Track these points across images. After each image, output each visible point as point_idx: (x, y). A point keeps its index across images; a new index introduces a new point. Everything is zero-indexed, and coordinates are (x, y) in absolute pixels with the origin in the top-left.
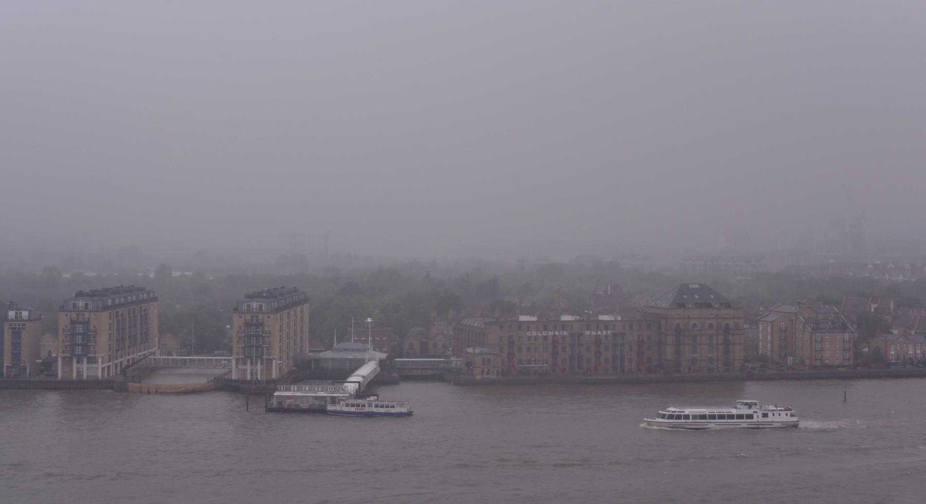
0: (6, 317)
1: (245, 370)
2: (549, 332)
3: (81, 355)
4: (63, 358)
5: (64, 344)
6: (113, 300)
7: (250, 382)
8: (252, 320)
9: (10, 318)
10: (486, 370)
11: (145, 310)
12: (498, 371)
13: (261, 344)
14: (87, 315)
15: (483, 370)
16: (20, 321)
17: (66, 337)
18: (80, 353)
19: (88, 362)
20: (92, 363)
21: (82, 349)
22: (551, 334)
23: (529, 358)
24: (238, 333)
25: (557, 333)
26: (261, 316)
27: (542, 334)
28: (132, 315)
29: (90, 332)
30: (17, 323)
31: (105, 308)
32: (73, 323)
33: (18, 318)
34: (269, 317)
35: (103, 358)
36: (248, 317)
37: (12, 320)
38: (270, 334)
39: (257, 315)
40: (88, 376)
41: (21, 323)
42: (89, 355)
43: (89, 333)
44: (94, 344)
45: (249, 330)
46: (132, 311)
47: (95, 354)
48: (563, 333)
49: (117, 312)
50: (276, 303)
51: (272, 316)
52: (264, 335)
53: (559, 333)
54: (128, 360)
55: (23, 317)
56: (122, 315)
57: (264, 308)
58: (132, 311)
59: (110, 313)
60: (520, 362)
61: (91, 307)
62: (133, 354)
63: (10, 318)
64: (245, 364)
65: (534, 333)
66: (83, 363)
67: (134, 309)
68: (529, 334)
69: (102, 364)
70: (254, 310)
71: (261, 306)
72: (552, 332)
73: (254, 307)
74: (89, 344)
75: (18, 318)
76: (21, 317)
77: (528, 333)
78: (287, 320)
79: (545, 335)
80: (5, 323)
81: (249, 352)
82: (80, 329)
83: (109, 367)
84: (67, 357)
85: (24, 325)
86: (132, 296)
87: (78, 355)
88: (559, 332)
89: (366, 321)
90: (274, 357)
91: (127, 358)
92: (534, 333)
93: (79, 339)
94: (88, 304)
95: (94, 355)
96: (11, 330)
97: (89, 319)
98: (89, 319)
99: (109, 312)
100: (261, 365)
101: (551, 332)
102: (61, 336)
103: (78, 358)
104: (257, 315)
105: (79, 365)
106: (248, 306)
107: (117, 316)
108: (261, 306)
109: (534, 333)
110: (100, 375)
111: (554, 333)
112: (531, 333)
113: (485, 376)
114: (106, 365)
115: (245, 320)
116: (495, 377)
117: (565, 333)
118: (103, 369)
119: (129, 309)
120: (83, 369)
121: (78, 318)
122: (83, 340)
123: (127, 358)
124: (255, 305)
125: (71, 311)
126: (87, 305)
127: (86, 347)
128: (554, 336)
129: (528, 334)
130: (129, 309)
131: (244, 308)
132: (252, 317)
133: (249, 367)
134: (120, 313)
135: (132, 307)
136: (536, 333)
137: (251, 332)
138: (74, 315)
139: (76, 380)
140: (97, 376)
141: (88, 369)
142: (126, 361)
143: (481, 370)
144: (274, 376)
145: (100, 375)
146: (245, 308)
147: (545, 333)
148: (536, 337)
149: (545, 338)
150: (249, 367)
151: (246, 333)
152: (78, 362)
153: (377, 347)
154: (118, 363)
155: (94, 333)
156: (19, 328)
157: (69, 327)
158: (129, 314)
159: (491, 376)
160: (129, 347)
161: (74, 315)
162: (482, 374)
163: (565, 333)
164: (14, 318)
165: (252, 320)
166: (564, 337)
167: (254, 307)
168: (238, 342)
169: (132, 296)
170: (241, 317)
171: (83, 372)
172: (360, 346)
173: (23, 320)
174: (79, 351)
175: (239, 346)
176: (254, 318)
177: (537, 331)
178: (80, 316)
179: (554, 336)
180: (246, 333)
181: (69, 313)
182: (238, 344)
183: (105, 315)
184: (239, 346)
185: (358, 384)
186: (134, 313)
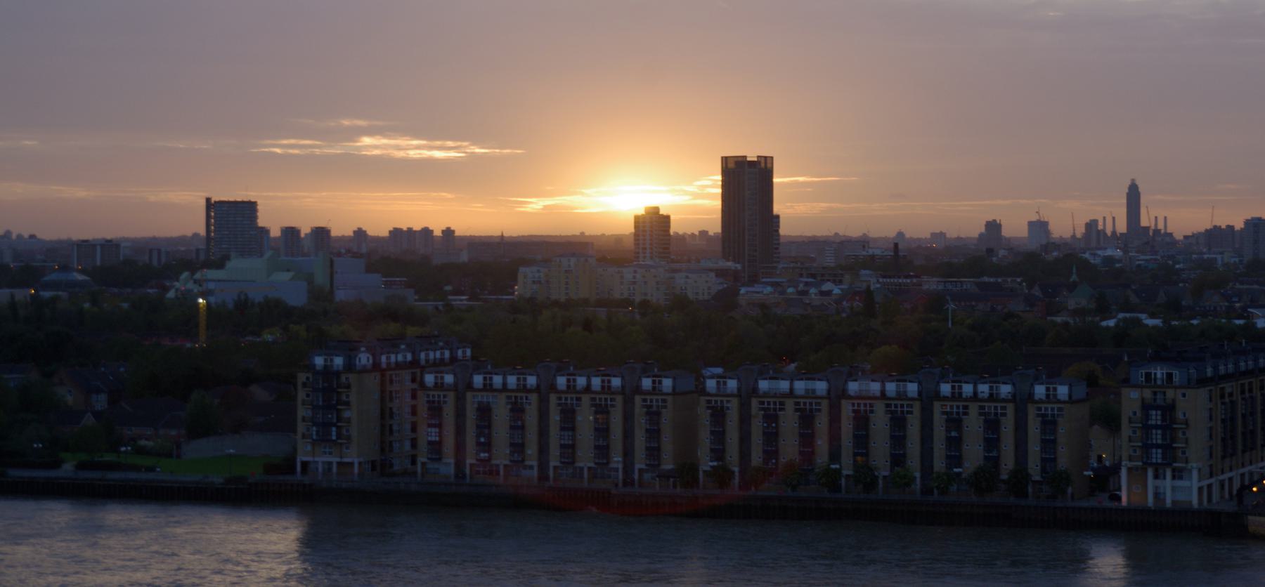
0: (1031, 395)
4: (1130, 470)
6: (1215, 368)
9: (1036, 397)
14: (1170, 393)
17: (1134, 432)
18: (1159, 461)
19: (1174, 477)
20: (1181, 478)
21: (1162, 453)
28: (1247, 395)
29: (1176, 424)
30: (1050, 406)
31: (1202, 382)
32: (1146, 407)
33: (1051, 397)
35: (1200, 470)
37: (1041, 401)
40: (1174, 502)
42: (1175, 465)
43: (1175, 426)
44: (1183, 445)
46: (1247, 387)
47: (1187, 462)
49: (1223, 389)
54: (1243, 475)
55: (1059, 397)
56: (1231, 395)
58: (1247, 387)
59: (1211, 390)
61: (1177, 380)
62: (1251, 464)
63: (1036, 397)
66: (1165, 478)
67: (1250, 383)
69: (1199, 481)
74: (1175, 445)
75: (1051, 397)
76: (1055, 396)
82: (1156, 417)
83: (1210, 486)
84: (1137, 468)
86: (1246, 362)
87: (1157, 464)
91: (1242, 471)
93: (1157, 437)
95: (1184, 465)
96: (1040, 419)
97: (1174, 400)
98: (1174, 400)
99: (1208, 388)
102: (1126, 431)
105: (1159, 482)
107: (1222, 396)
110: (1195, 502)
114: (1205, 483)
118: (1200, 489)
119: (1243, 385)
121: (1155, 400)
122: (1164, 438)
123: (1242, 471)
125: (1142, 387)
126: (1170, 376)
127: (1168, 448)
130: (1243, 385)
134: (1228, 390)
135: (1246, 381)
138: (1148, 394)
139: (1153, 508)
140: (1191, 502)
141: (1174, 489)
142: (1239, 477)
145: (1195, 502)
152: (1156, 477)
154: (1224, 480)
155: (1184, 426)
157: (1139, 414)
158: (1243, 392)
160: (1244, 452)
161: (1148, 394)
164: (1044, 397)
169: (1246, 362)
171: (1164, 493)
173: (1060, 402)
174: (1157, 456)
178: (1158, 396)
183: (1202, 394)
186: (1251, 390)
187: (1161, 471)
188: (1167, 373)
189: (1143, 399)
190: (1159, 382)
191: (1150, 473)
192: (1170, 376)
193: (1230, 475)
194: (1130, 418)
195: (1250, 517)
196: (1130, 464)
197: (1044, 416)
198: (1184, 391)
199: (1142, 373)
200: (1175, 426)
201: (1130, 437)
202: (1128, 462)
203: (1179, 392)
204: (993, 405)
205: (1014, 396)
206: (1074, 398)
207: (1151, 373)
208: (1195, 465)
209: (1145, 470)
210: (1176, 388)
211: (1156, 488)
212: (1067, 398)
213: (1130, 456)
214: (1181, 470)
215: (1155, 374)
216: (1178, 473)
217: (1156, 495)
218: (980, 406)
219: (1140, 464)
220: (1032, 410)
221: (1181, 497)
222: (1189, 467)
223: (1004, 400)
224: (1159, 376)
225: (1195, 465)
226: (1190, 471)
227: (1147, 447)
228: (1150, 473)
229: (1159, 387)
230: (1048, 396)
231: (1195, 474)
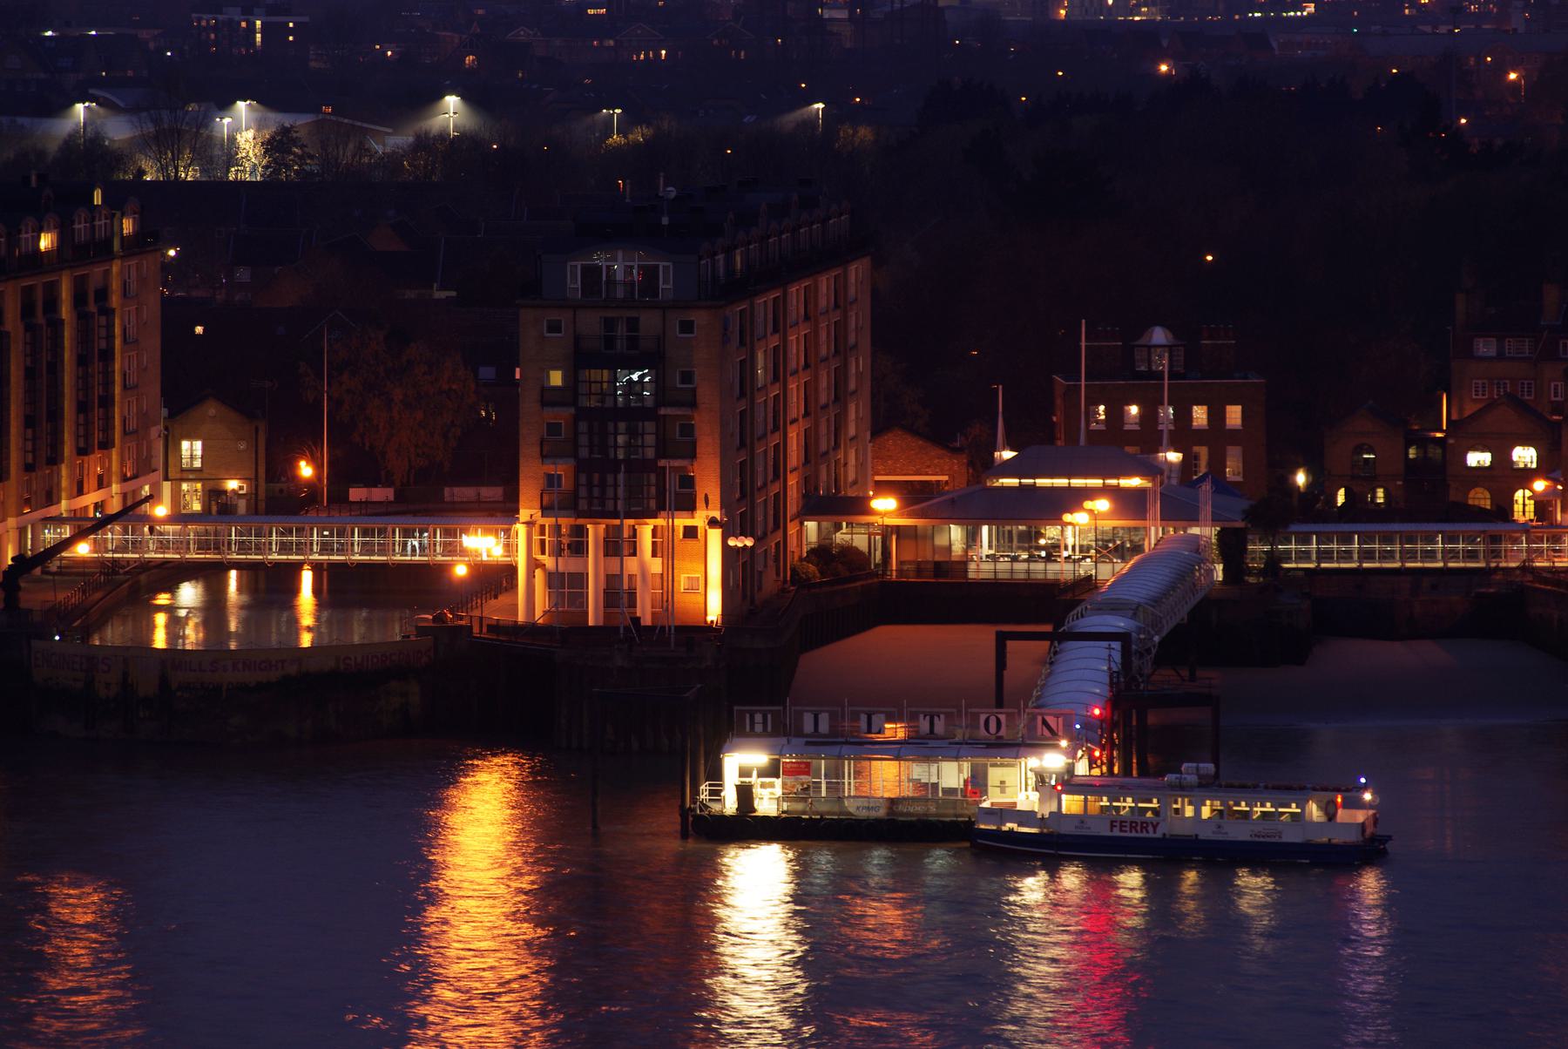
7: (605, 632)
8: (609, 341)
13: (650, 453)
26: (649, 322)
28: (40, 319)
34: (687, 327)
36: (591, 323)
39: (633, 314)
46: (39, 295)
50: (721, 257)
51: (700, 318)
52: (663, 411)
57: (665, 285)
58: (39, 295)
70: (620, 294)
71: (650, 274)
73: (620, 276)
78: (774, 341)
81: (596, 492)
89: (1141, 342)
104: (633, 314)
106: (591, 273)
108: (650, 274)
115: (577, 339)
124: (619, 265)
130: (28, 292)
131: (570, 285)
132: (609, 324)
165: (609, 341)
170: (554, 327)
176: (621, 330)
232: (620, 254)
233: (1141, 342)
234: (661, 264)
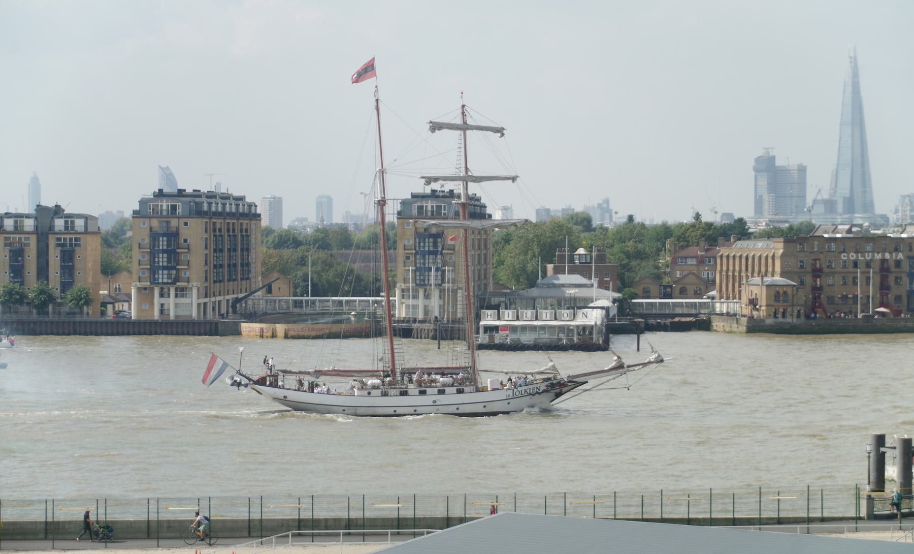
0: (51, 228)
1: (415, 307)
2: (876, 254)
3: (167, 283)
5: (141, 267)
9: (57, 229)
10: (781, 310)
11: (246, 230)
12: (799, 311)
14: (174, 223)
15: (776, 310)
16: (71, 234)
17: (144, 257)
18: (165, 281)
19: (176, 296)
20: (183, 296)
22: (878, 257)
23: (844, 294)
24: (405, 249)
25: (887, 256)
27: (865, 257)
29: (179, 248)
30: (68, 236)
32: (154, 236)
37: (60, 233)
38: (454, 250)
40: (176, 316)
41: (73, 236)
42: (178, 284)
43: (178, 250)
44: (186, 267)
45: (422, 244)
47: (188, 282)
48: (897, 257)
53: (891, 256)
60: (831, 300)
61: (180, 211)
63: (57, 229)
64: (415, 297)
65: (853, 256)
66: (169, 296)
68: (844, 256)
71: (439, 207)
72: (880, 254)
76: (73, 227)
77: (843, 254)
79: (869, 258)
80: (50, 236)
82: (163, 243)
83: (205, 304)
84: (145, 289)
85: (76, 239)
87: (163, 283)
88: (891, 253)
90: (460, 286)
92: (853, 256)
93: (162, 260)
94: (176, 206)
96: (60, 248)
97: (178, 228)
98: (178, 228)
99: (205, 220)
100: (440, 298)
101: (878, 253)
103: (162, 289)
105: (163, 300)
109: (853, 256)
110: (194, 314)
111: (884, 255)
112: (848, 257)
113: (781, 320)
116: (795, 320)
117: (900, 256)
118: (199, 305)
120: (169, 304)
122: (169, 261)
125: (150, 218)
126: (174, 208)
128: (883, 261)
129: (843, 257)
133: (421, 302)
136: (855, 255)
137: (424, 247)
139: (160, 321)
141: (176, 305)
143: (774, 310)
144: (459, 315)
146: (415, 212)
147: (868, 257)
148: (855, 264)
149: (868, 265)
150: (421, 302)
151: (417, 248)
152: (162, 295)
153: (603, 285)
155: (186, 250)
156: (71, 245)
157: (147, 241)
159: (789, 319)
162: (775, 317)
163: (900, 256)
164: (63, 229)
166: (898, 263)
167: (429, 208)
168: (404, 262)
171: (169, 310)
172: (578, 279)
173: (77, 233)
175: (406, 268)
177: (857, 252)
179: (883, 261)
180: (417, 248)
181: (147, 221)
182: (405, 266)
184: (406, 268)
185: (604, 312)
187: (166, 290)
188: (171, 205)
189: (151, 229)
190: (165, 213)
191: (157, 291)
192: (174, 208)
193: (207, 300)
194: (139, 244)
195: (243, 325)
196: (139, 285)
197: (63, 245)
198: (185, 220)
199: (150, 205)
200: (178, 250)
201: (139, 261)
202: (138, 283)
203: (182, 221)
204: (17, 236)
205: (37, 227)
206: (89, 230)
207: (158, 205)
208: (195, 284)
209: (152, 290)
210: (179, 218)
211: (162, 305)
212: (82, 229)
213: (139, 277)
214: (183, 289)
215: (161, 206)
216: (181, 292)
217: (162, 311)
218: (5, 238)
219: (149, 283)
220: (52, 241)
221: (183, 312)
222: (190, 286)
223: (28, 233)
224: (165, 207)
225: (195, 284)
226: (191, 289)
227: (153, 270)
228: (157, 291)
229: (165, 217)
230: (66, 228)
231: (195, 291)
232: (430, 201)
233: (576, 253)
234: (443, 205)
